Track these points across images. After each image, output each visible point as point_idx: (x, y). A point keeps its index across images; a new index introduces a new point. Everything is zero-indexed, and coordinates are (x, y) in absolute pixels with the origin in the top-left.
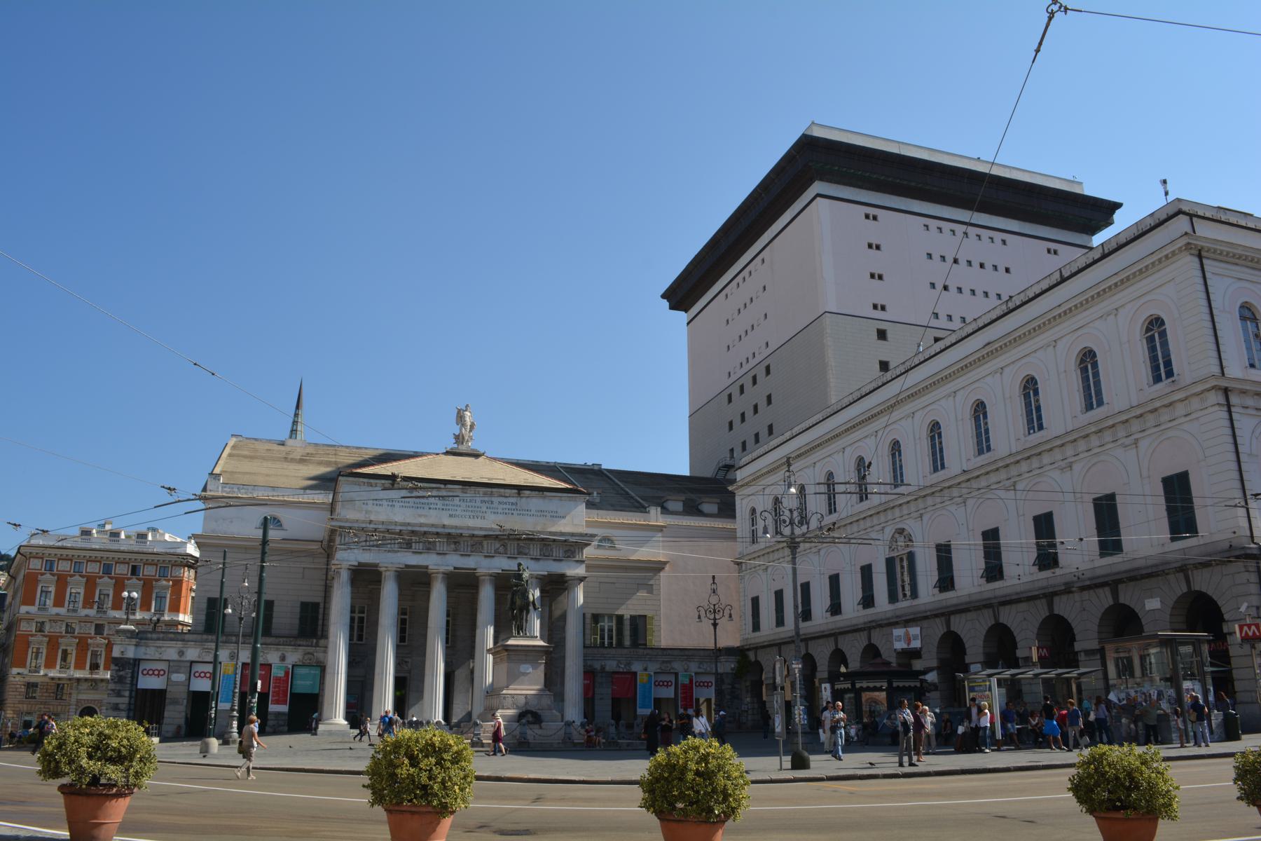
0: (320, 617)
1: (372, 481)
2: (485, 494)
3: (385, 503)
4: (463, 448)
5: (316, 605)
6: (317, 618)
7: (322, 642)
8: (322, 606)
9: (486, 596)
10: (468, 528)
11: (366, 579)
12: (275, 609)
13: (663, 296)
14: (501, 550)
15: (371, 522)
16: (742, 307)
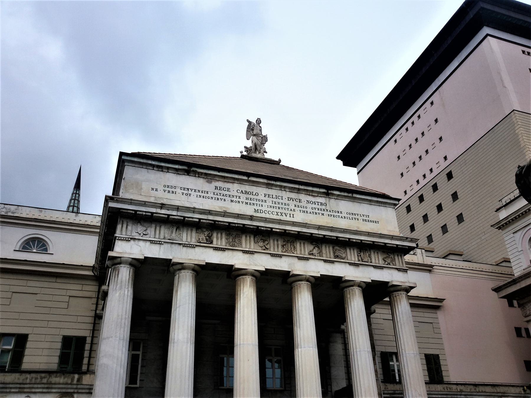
0: (86, 354)
1: (163, 164)
2: (292, 190)
3: (178, 191)
4: (258, 155)
5: (81, 340)
6: (83, 354)
7: (86, 379)
8: (89, 340)
9: (304, 306)
10: (280, 222)
11: (153, 281)
12: (29, 345)
13: (338, 158)
14: (315, 251)
15: (163, 206)
16: (413, 142)
